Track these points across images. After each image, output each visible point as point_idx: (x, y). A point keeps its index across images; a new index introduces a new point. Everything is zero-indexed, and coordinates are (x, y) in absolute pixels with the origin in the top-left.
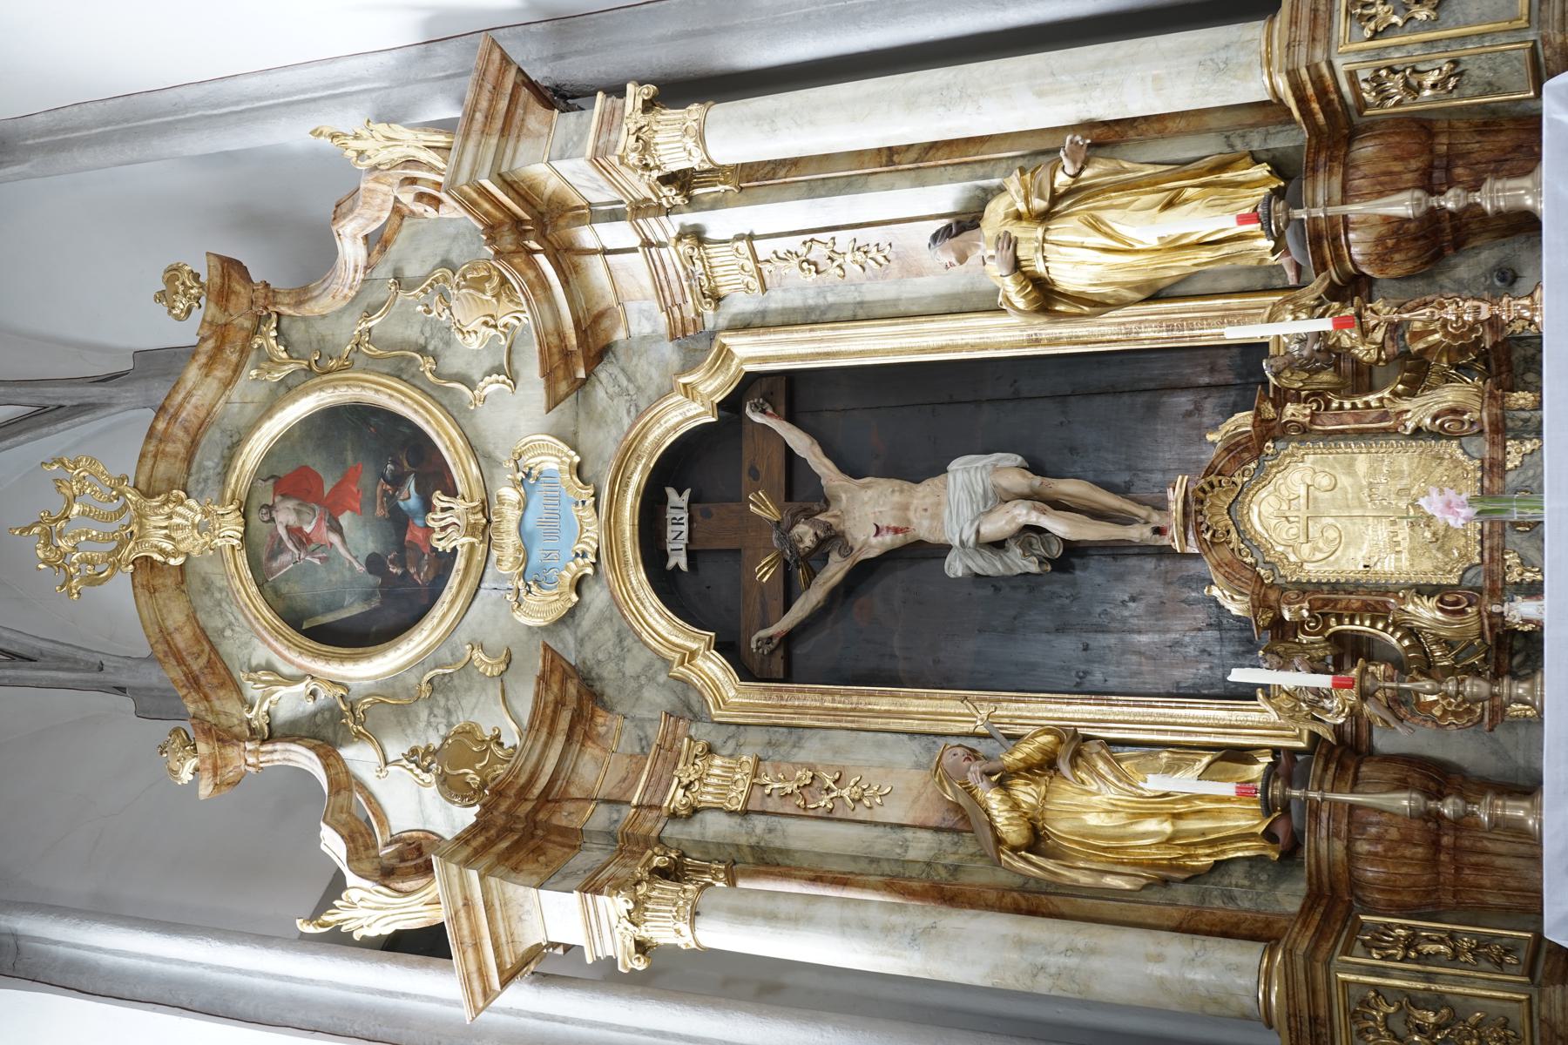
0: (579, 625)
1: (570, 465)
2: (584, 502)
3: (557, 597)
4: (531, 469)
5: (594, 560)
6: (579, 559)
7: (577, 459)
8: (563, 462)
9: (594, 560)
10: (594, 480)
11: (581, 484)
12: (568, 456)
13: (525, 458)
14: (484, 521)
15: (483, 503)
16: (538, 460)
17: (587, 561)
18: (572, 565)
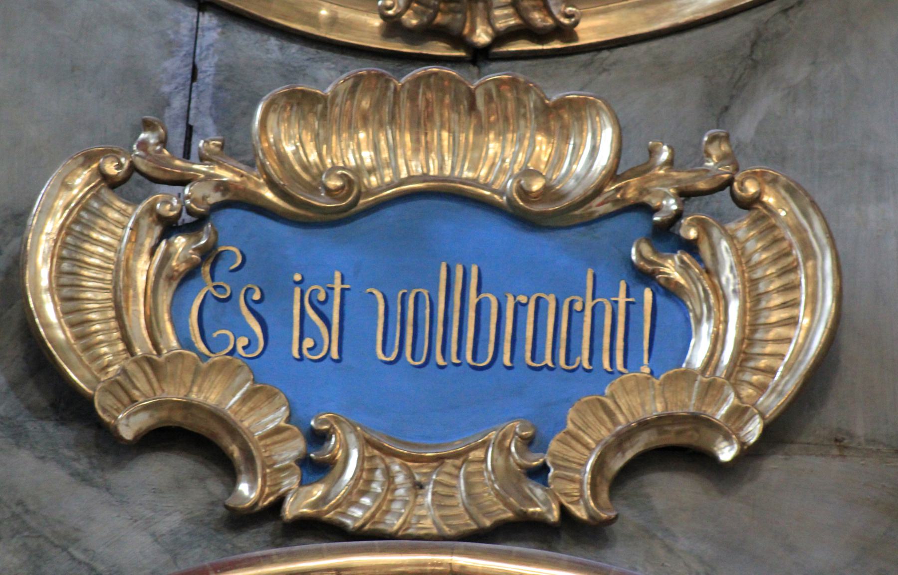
0: (19, 436)
1: (699, 421)
2: (539, 473)
3: (143, 346)
4: (691, 247)
5: (290, 511)
6: (295, 447)
7: (726, 453)
8: (712, 390)
9: (290, 511)
10: (630, 517)
11: (617, 463)
12: (740, 413)
13: (742, 227)
14: (482, 37)
15: (564, 32)
16: (729, 278)
17: (290, 482)
18: (277, 417)
